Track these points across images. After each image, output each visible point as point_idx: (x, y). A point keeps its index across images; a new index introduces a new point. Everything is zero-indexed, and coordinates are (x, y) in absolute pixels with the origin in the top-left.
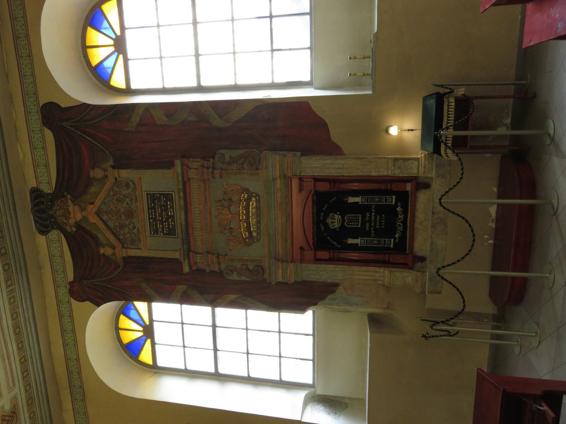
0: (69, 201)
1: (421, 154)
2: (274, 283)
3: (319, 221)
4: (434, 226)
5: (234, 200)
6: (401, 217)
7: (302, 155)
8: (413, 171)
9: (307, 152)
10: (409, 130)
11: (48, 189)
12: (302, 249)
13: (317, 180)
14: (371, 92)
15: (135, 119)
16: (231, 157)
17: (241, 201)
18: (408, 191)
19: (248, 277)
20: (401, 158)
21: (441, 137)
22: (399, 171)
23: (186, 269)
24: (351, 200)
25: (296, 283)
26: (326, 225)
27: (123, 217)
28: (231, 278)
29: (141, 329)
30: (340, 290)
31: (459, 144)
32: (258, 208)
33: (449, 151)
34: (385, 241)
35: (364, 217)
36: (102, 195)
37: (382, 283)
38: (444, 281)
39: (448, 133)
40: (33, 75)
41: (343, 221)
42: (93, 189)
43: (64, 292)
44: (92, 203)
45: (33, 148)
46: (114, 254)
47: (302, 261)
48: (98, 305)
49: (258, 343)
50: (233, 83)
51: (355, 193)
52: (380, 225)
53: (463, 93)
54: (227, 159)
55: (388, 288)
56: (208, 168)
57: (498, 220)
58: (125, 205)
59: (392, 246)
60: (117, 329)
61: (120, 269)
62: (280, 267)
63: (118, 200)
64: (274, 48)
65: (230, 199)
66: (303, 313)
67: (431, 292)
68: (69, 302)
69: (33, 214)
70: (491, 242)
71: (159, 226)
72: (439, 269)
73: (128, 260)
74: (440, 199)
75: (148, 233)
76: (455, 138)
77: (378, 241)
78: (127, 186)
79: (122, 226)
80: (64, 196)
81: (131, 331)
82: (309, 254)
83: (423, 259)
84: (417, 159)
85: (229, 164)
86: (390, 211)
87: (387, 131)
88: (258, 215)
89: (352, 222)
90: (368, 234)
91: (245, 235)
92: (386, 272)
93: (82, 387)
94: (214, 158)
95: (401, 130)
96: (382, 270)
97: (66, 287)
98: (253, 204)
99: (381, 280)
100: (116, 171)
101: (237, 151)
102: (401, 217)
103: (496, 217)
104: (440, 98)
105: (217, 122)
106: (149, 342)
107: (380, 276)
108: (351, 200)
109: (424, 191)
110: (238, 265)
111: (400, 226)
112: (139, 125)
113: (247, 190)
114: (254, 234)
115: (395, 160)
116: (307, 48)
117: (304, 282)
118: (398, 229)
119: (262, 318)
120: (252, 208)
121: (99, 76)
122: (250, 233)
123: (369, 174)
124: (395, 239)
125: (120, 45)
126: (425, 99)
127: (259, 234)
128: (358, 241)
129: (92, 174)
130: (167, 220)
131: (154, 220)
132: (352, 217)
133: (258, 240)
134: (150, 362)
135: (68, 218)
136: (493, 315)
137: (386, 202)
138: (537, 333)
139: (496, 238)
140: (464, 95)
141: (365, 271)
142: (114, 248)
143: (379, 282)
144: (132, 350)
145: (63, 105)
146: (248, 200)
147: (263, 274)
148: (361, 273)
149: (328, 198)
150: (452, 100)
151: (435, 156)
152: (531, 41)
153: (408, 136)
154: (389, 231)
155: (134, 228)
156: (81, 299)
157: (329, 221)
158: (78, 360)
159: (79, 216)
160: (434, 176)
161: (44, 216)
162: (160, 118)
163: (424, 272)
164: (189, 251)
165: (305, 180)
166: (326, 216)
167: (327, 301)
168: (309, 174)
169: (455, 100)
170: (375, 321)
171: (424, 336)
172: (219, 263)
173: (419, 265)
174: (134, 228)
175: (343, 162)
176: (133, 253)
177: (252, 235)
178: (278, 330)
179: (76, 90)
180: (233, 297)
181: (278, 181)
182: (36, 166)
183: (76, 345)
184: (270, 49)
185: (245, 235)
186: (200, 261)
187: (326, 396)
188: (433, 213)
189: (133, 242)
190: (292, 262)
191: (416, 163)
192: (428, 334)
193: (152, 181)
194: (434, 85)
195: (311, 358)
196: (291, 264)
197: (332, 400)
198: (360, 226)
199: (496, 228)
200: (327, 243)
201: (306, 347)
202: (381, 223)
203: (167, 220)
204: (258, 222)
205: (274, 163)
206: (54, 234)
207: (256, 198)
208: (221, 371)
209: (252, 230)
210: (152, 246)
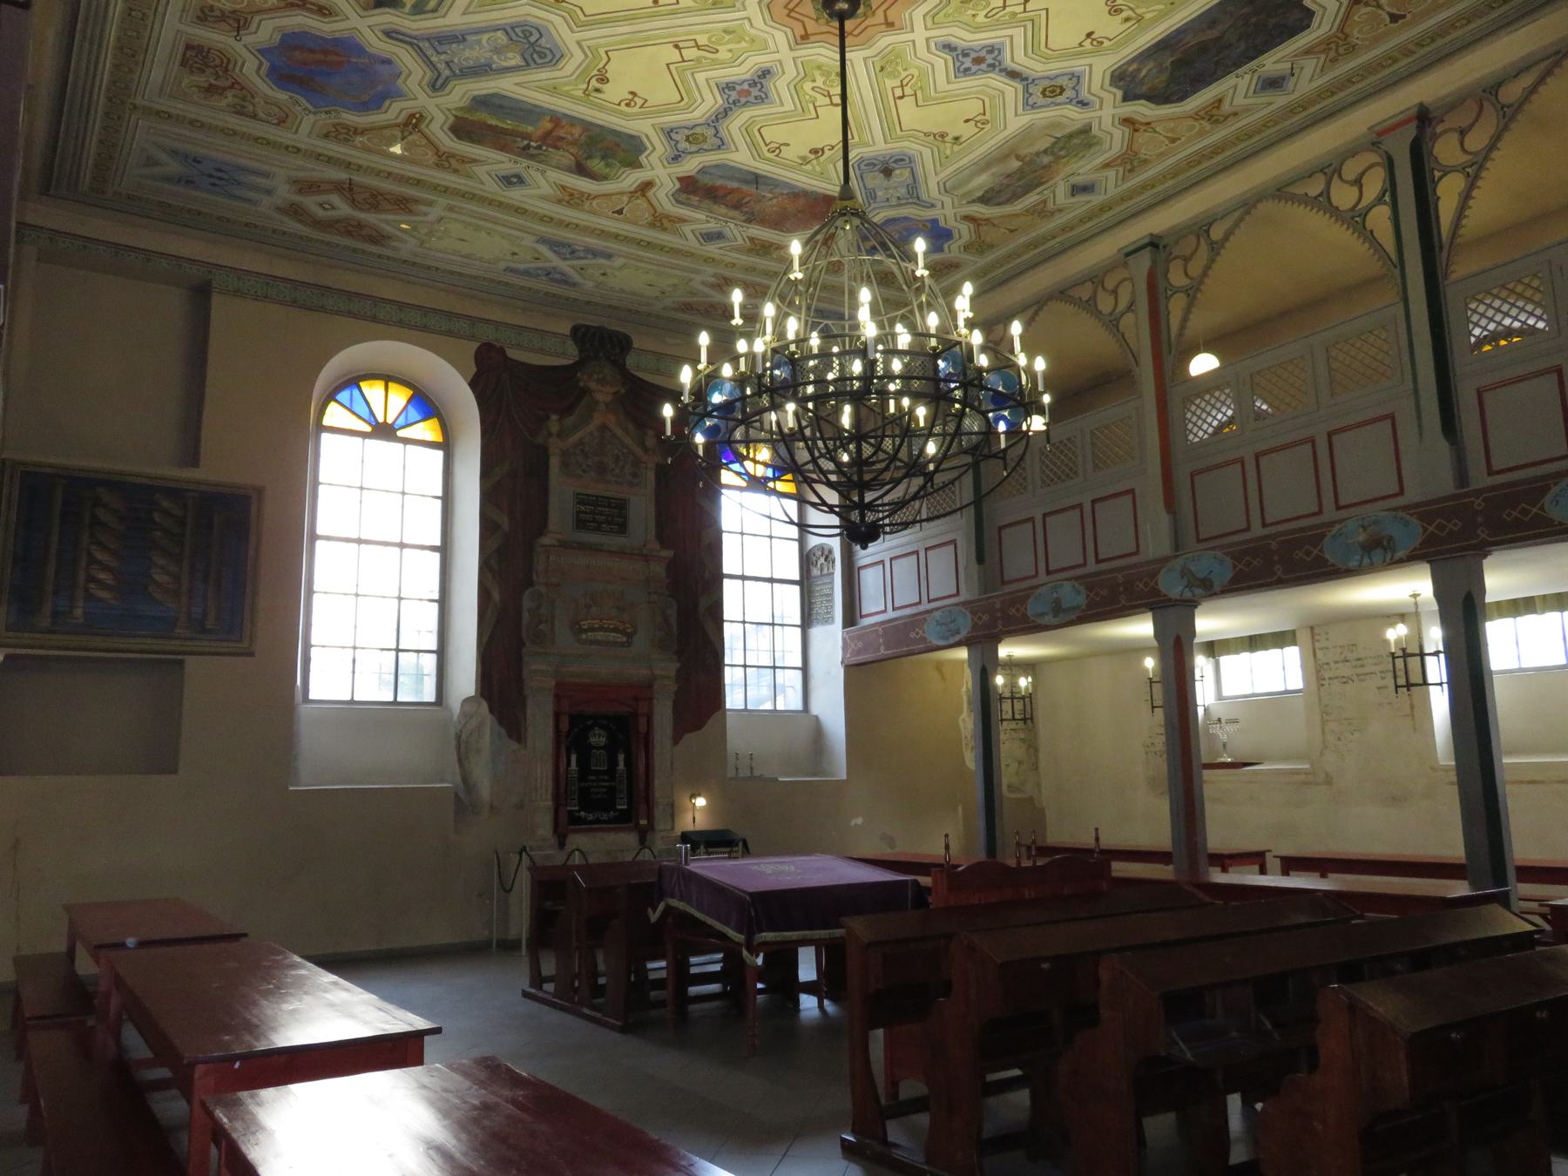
8: (661, 824)
20: (672, 811)
30: (515, 745)
32: (615, 643)
75: (579, 490)
122: (586, 631)
127: (585, 642)
130: (594, 520)
200: (573, 732)
203: (594, 520)
204: (598, 643)
205: (666, 669)
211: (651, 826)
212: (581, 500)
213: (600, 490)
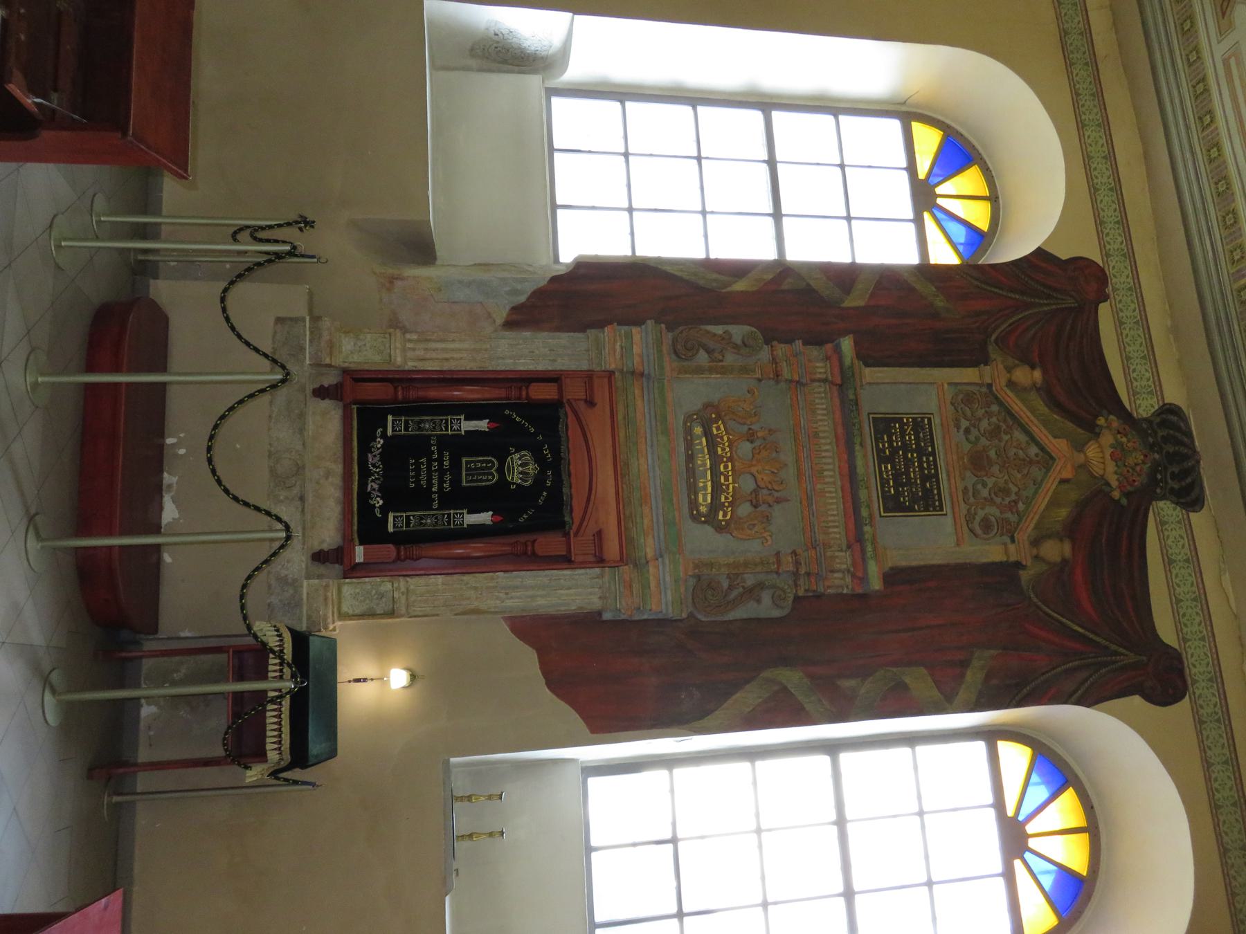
0: (1114, 484)
1: (334, 630)
2: (650, 323)
3: (553, 464)
4: (299, 469)
5: (748, 504)
6: (372, 486)
7: (600, 613)
8: (352, 592)
9: (588, 621)
10: (365, 680)
11: (1164, 509)
12: (591, 403)
13: (565, 561)
14: (453, 760)
15: (973, 677)
16: (759, 601)
17: (731, 504)
18: (361, 544)
19: (708, 332)
21: (293, 676)
22: (383, 589)
23: (847, 344)
24: (485, 518)
25: (601, 325)
26: (540, 459)
27: (992, 454)
28: (747, 328)
29: (940, 201)
30: (501, 315)
31: (252, 658)
32: (693, 489)
33: (273, 642)
34: (406, 429)
35: (456, 481)
36: (1042, 502)
37: (408, 336)
38: (268, 351)
39: (278, 682)
40: (1207, 764)
41: (501, 471)
42: (1063, 513)
43: (1119, 278)
44: (1063, 481)
45: (1201, 598)
46: (1009, 370)
47: (588, 377)
48: (1039, 252)
49: (678, 185)
50: (760, 764)
51: (477, 532)
52: (418, 465)
53: (249, 773)
54: (766, 597)
55: (395, 324)
56: (808, 574)
57: (158, 489)
58: (990, 482)
59: (390, 418)
60: (993, 198)
61: (994, 337)
62: (637, 360)
63: (1006, 492)
64: (670, 846)
65: (756, 507)
66: (581, 257)
67: (295, 320)
68: (1106, 255)
69: (1195, 451)
70: (169, 441)
71: (910, 438)
72: (283, 381)
73: (978, 358)
74: (288, 538)
75: (936, 421)
76: (262, 675)
77: (420, 429)
78: (986, 525)
79: (995, 433)
80: (1128, 495)
81: (963, 194)
82: (574, 391)
83: (321, 393)
84: (343, 616)
85: (761, 586)
86: (397, 497)
87: (413, 677)
88: (691, 473)
89: (481, 468)
90: (444, 442)
91: (718, 429)
92: (399, 359)
93: (1069, 64)
94: (797, 599)
95: (382, 679)
96: (410, 365)
97: (1114, 290)
98: (704, 499)
99: (410, 341)
100: (1013, 559)
101: (745, 616)
102: (372, 486)
103: (162, 497)
104: (300, 757)
105: (792, 678)
106: (922, 174)
107: (414, 350)
108: (485, 518)
109: (325, 547)
110: (730, 358)
111: (374, 465)
112: (964, 664)
113: (719, 528)
114: (698, 430)
115: (391, 614)
116: (596, 849)
117: (583, 328)
118: (378, 458)
119: (670, 241)
120: (705, 488)
121: (1057, 767)
122: (707, 433)
123: (449, 578)
124: (384, 435)
125: (1014, 838)
126: (332, 753)
127: (688, 431)
128: (467, 426)
129: (1067, 548)
130: (894, 451)
131: (925, 450)
132: (481, 480)
133: (689, 418)
134: (917, 127)
135: (1118, 446)
136: (156, 277)
137: (408, 517)
138: (59, 247)
139: (161, 447)
140: (247, 767)
141: (447, 359)
142: (1011, 384)
143: (415, 337)
144: (958, 153)
145: (1137, 700)
146: (715, 506)
147: (675, 342)
148: (455, 356)
149: (535, 520)
150: (272, 756)
151: (303, 627)
152: (106, 908)
153: (365, 667)
154: (398, 451)
155: (967, 431)
156: (1079, 263)
157: (533, 468)
158: (1081, 126)
159: (1092, 451)
160: (305, 583)
161: (1171, 448)
162: (918, 681)
163: (317, 365)
164: (844, 384)
165: (591, 558)
166: (539, 481)
167: (529, 288)
168: (582, 571)
169: (265, 755)
170: (420, 247)
171: (309, 224)
172: (774, 361)
173: (330, 380)
174: (967, 431)
175: (509, 603)
176: (968, 375)
177: (703, 427)
178: (635, 213)
179: (1109, 734)
180: (740, 286)
181: (650, 553)
182: (1194, 559)
183: (1087, 159)
184: (680, 844)
185: (718, 429)
186: (817, 362)
187: (520, 72)
188: (302, 499)
189: (969, 399)
190: (610, 374)
191: (345, 609)
192: (301, 229)
193: (932, 540)
194: (313, 784)
195: (557, 155)
196: (613, 367)
197: (505, 62)
198: (464, 460)
199: (161, 472)
200: (533, 417)
201: (571, 179)
202: (418, 470)
203: (894, 451)
204: (690, 458)
205: (662, 593)
206: (1145, 407)
207: (698, 511)
208: (757, 116)
209: (704, 440)
210: (924, 391)
211: (353, 571)
212: (920, 425)
213: (945, 460)
